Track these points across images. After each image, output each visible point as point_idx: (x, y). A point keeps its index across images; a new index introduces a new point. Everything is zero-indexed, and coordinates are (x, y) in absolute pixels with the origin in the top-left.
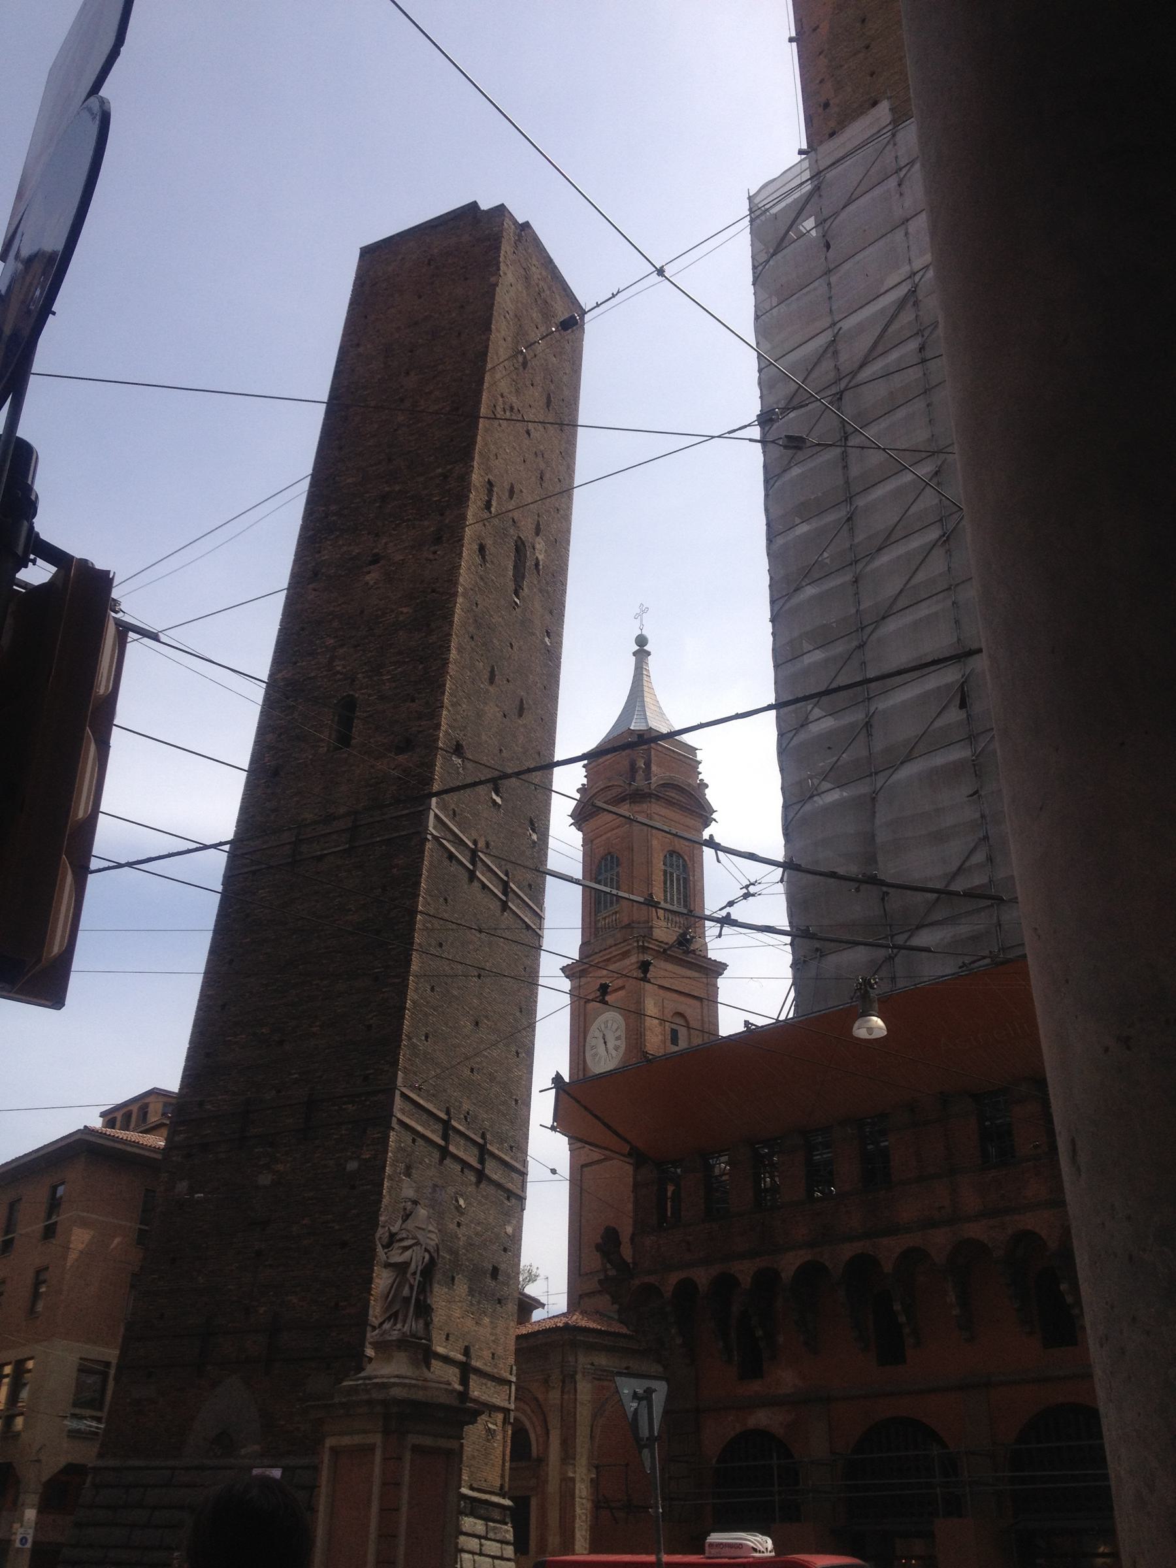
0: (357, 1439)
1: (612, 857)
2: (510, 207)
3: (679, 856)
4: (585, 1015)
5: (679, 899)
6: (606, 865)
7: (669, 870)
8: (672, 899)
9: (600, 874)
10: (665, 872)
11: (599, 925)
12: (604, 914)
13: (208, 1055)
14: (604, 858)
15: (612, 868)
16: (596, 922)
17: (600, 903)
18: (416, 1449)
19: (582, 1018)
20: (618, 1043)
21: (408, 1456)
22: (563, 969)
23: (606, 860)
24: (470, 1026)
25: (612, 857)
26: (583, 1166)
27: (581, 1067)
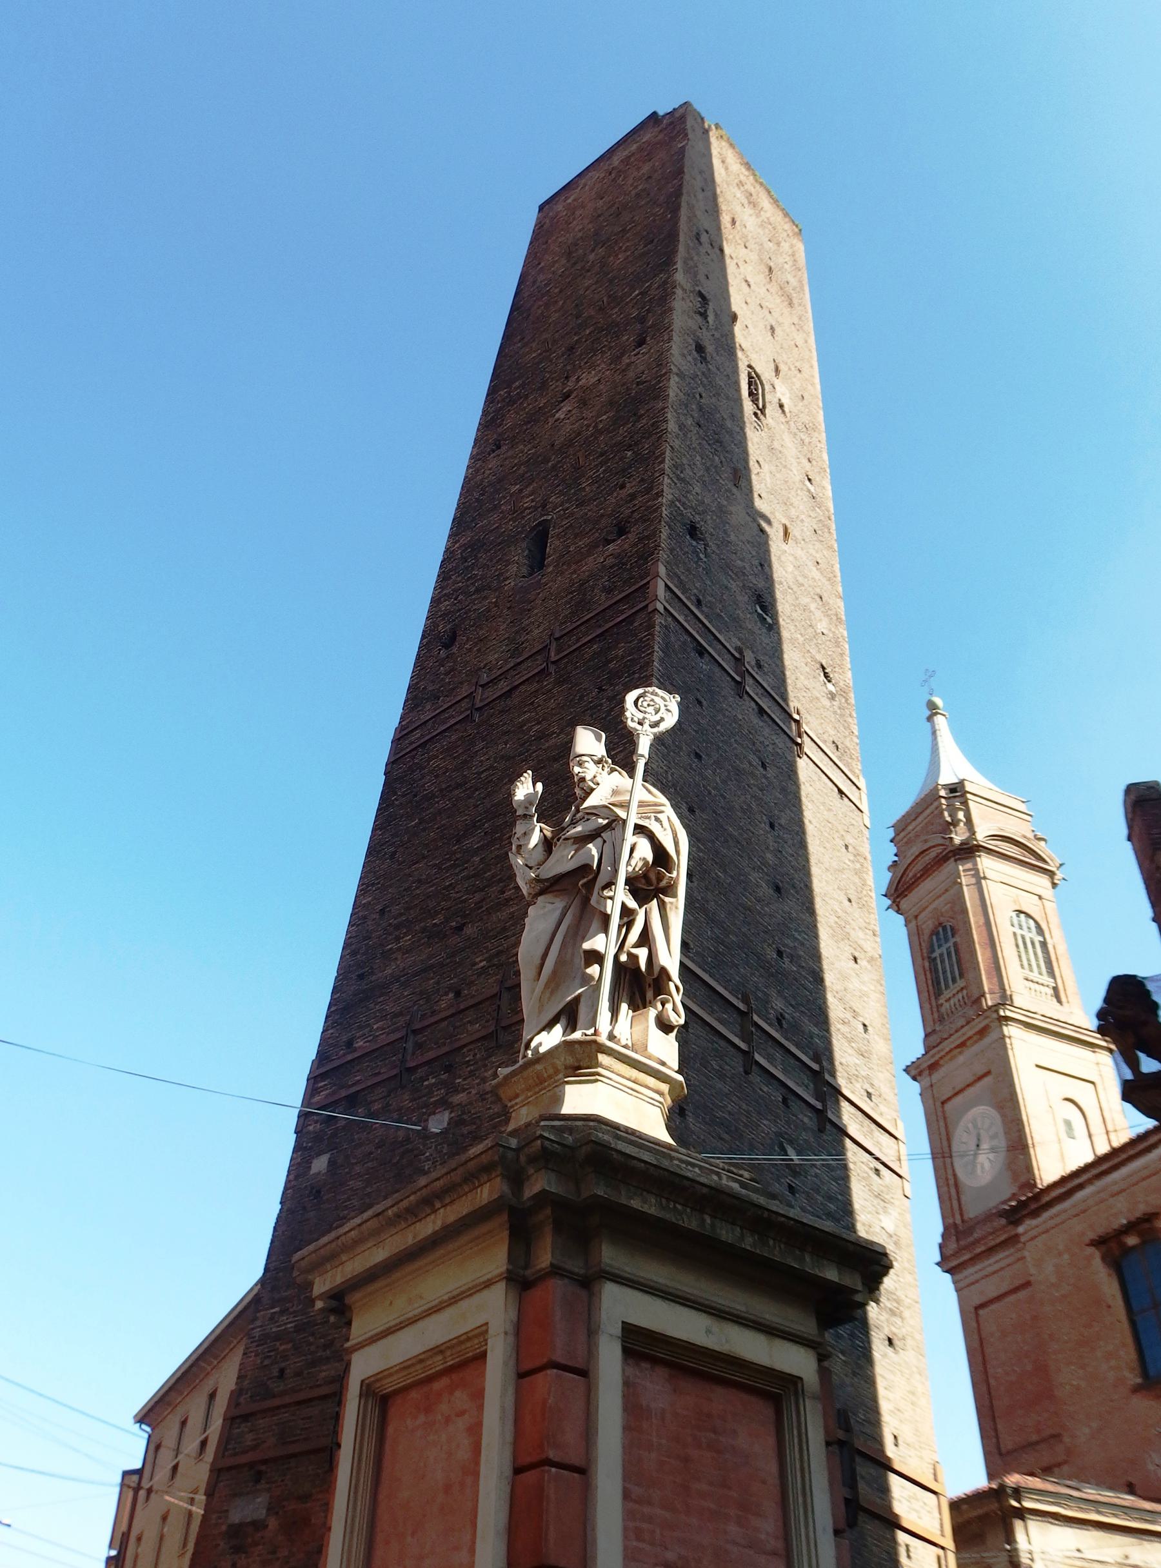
0: (437, 1331)
1: (944, 928)
2: (698, 106)
3: (1028, 916)
4: (945, 1118)
5: (1038, 966)
6: (938, 940)
7: (1019, 932)
8: (1030, 965)
9: (933, 951)
10: (1015, 934)
11: (943, 1010)
12: (947, 994)
13: (361, 977)
14: (935, 933)
15: (947, 940)
16: (939, 1006)
17: (939, 983)
18: (641, 1345)
19: (942, 1123)
20: (995, 1143)
21: (609, 1360)
22: (907, 1070)
23: (937, 934)
24: (766, 890)
25: (944, 928)
26: (977, 1308)
27: (952, 1182)
